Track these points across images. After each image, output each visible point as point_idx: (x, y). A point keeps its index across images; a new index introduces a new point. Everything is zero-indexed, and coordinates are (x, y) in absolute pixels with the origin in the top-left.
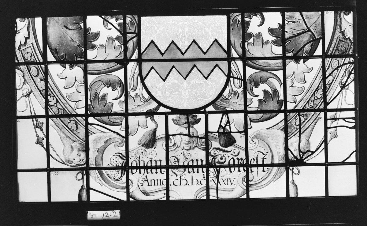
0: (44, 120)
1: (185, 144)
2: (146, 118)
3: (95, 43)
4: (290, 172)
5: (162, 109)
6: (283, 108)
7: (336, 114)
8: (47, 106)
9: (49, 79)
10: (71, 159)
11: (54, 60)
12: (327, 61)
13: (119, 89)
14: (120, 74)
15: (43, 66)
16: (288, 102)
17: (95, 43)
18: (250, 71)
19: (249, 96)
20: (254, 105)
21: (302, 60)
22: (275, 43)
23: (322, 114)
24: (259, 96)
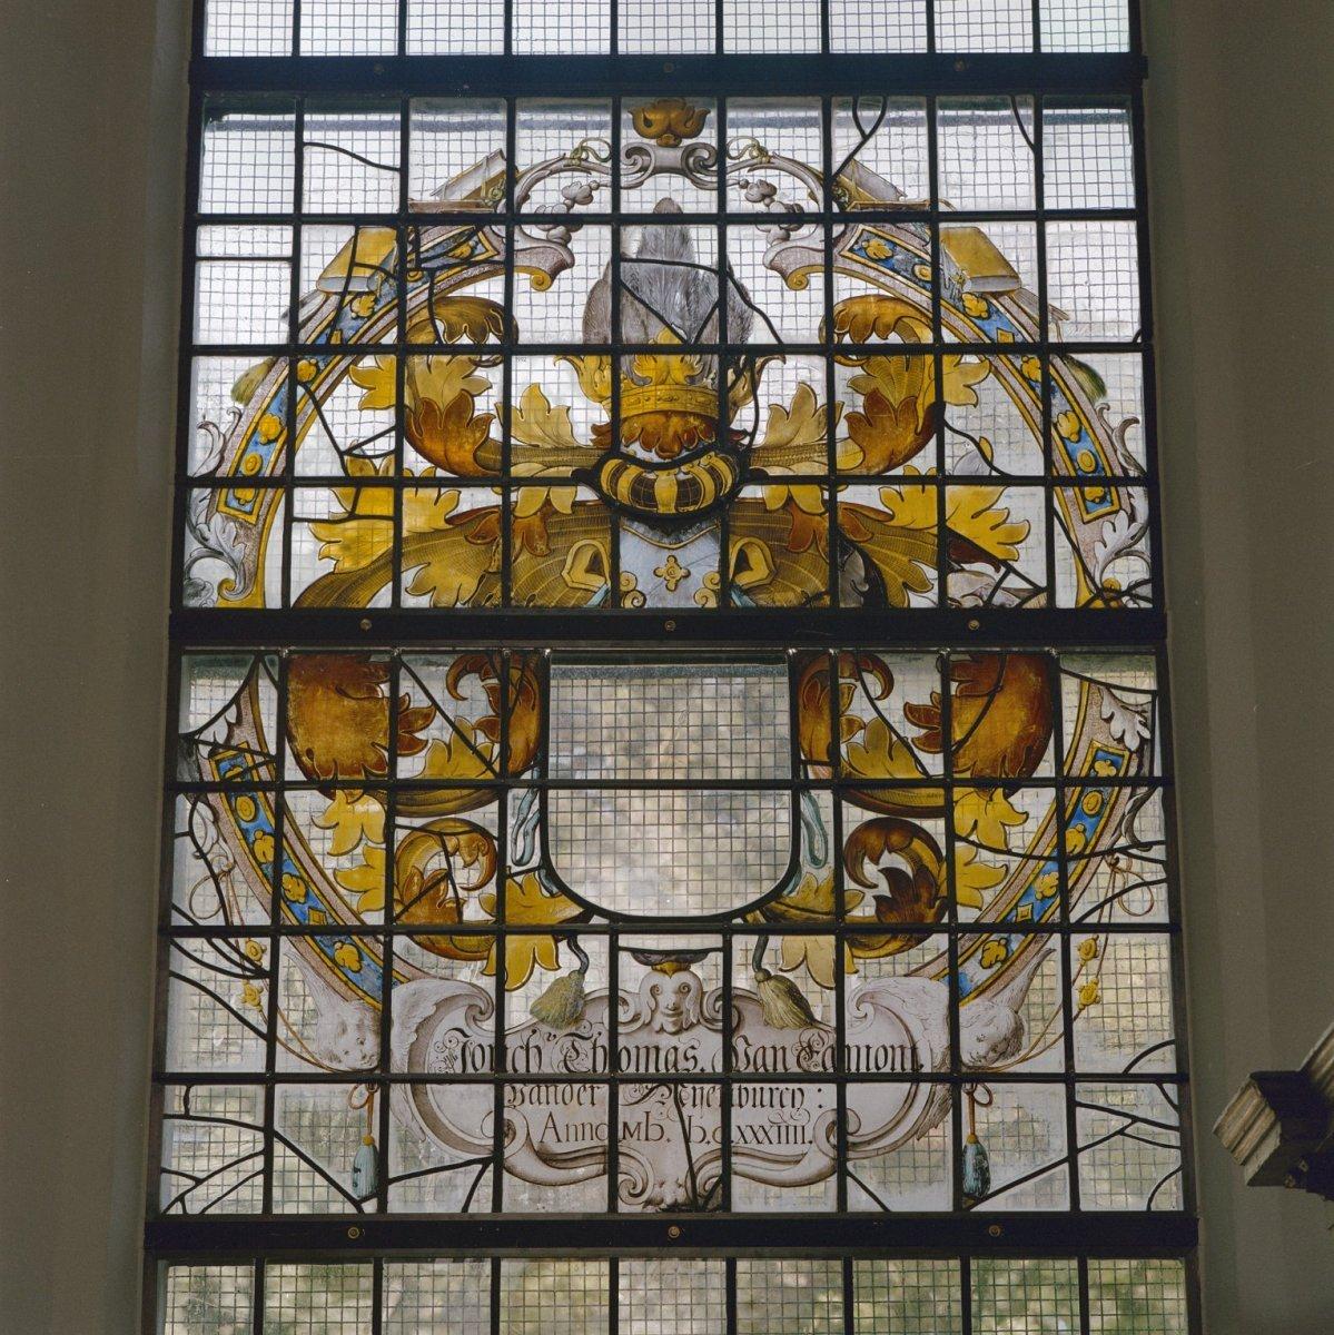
0: (266, 942)
1: (668, 1015)
2: (557, 941)
3: (420, 735)
4: (965, 1099)
5: (596, 920)
6: (945, 920)
7: (1095, 940)
8: (277, 900)
9: (287, 827)
10: (339, 1052)
11: (301, 777)
12: (1072, 793)
13: (483, 860)
14: (487, 815)
15: (271, 796)
16: (962, 905)
17: (420, 735)
18: (855, 816)
19: (849, 884)
20: (864, 911)
21: (1000, 791)
22: (928, 743)
23: (1055, 941)
24: (875, 886)
